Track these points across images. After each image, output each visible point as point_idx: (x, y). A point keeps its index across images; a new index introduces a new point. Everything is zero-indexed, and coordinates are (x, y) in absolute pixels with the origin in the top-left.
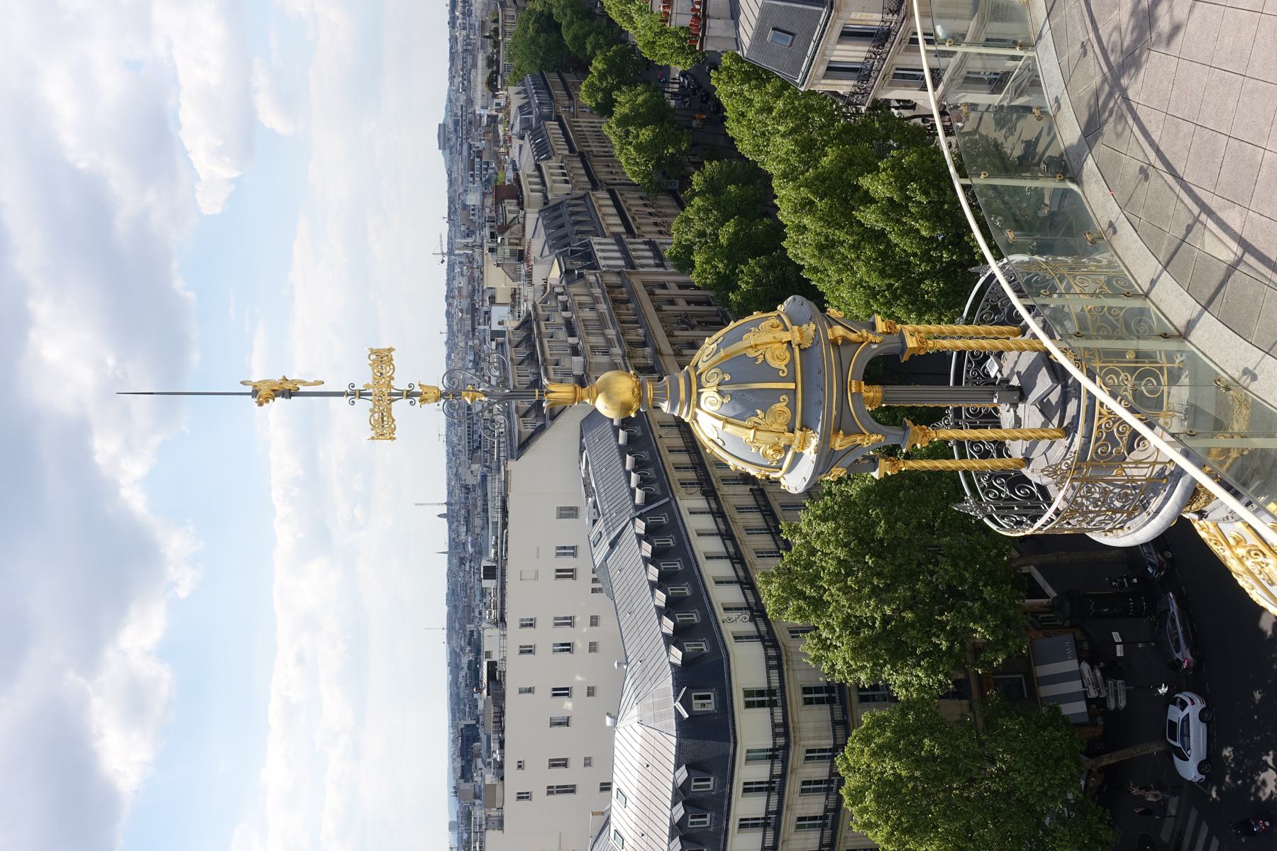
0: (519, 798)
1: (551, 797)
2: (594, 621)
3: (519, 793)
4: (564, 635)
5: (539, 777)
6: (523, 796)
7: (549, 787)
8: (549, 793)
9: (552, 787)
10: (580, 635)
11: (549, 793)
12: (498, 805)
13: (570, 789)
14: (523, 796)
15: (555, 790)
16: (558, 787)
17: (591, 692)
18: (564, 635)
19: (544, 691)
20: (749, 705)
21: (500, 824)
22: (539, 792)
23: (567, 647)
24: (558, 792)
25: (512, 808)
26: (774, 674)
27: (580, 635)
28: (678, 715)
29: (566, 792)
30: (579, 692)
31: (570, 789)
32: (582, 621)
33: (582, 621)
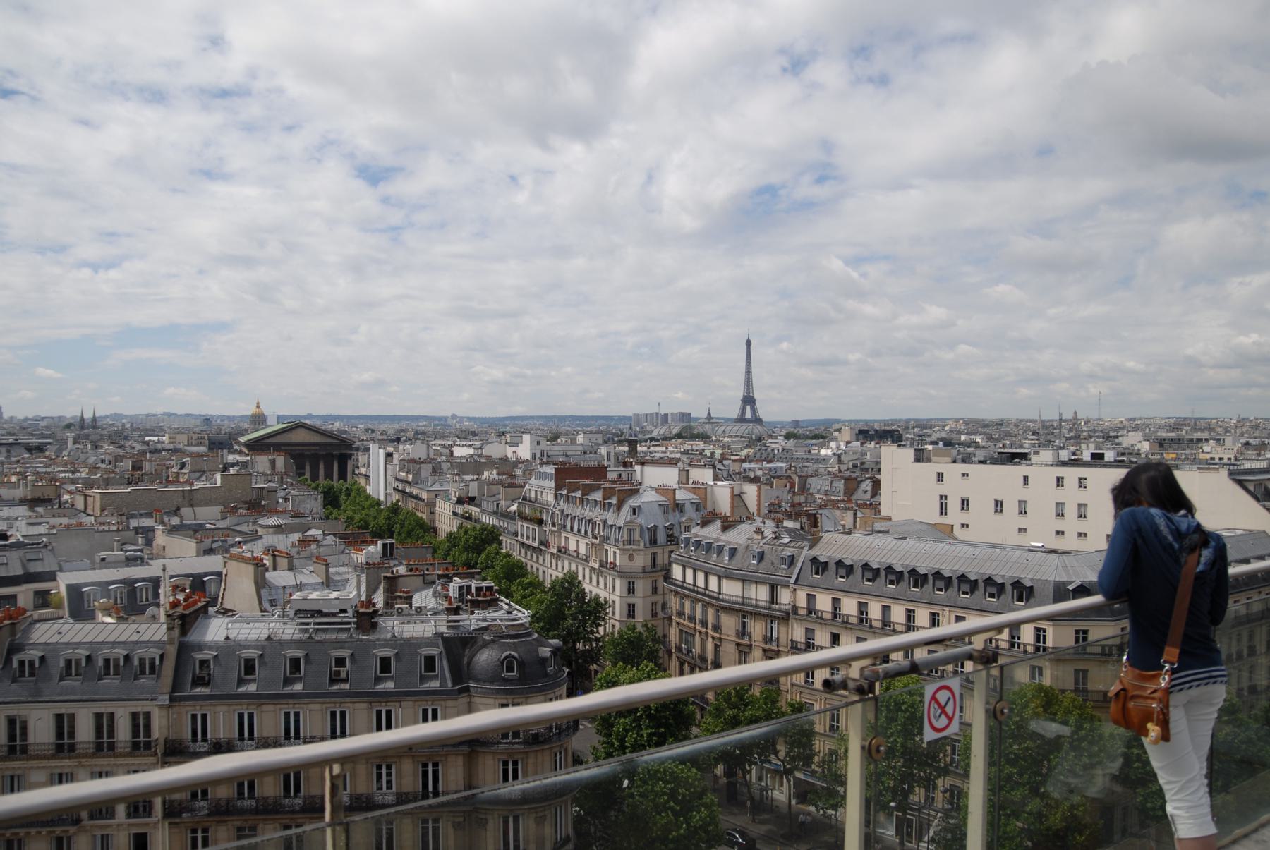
0: (939, 474)
1: (938, 498)
2: (1082, 535)
3: (942, 474)
4: (1071, 511)
5: (955, 488)
6: (940, 477)
7: (946, 497)
8: (941, 497)
9: (946, 499)
10: (1071, 523)
11: (941, 497)
12: (934, 459)
13: (943, 510)
14: (940, 477)
15: (944, 501)
16: (946, 503)
17: (1022, 530)
18: (1071, 511)
19: (1024, 494)
20: (1077, 632)
21: (917, 460)
22: (942, 489)
23: (1060, 515)
24: (942, 503)
25: (929, 469)
26: (1099, 650)
27: (1071, 523)
28: (1072, 582)
29: (942, 508)
30: (1023, 522)
31: (943, 510)
32: (1082, 526)
33: (1082, 526)
